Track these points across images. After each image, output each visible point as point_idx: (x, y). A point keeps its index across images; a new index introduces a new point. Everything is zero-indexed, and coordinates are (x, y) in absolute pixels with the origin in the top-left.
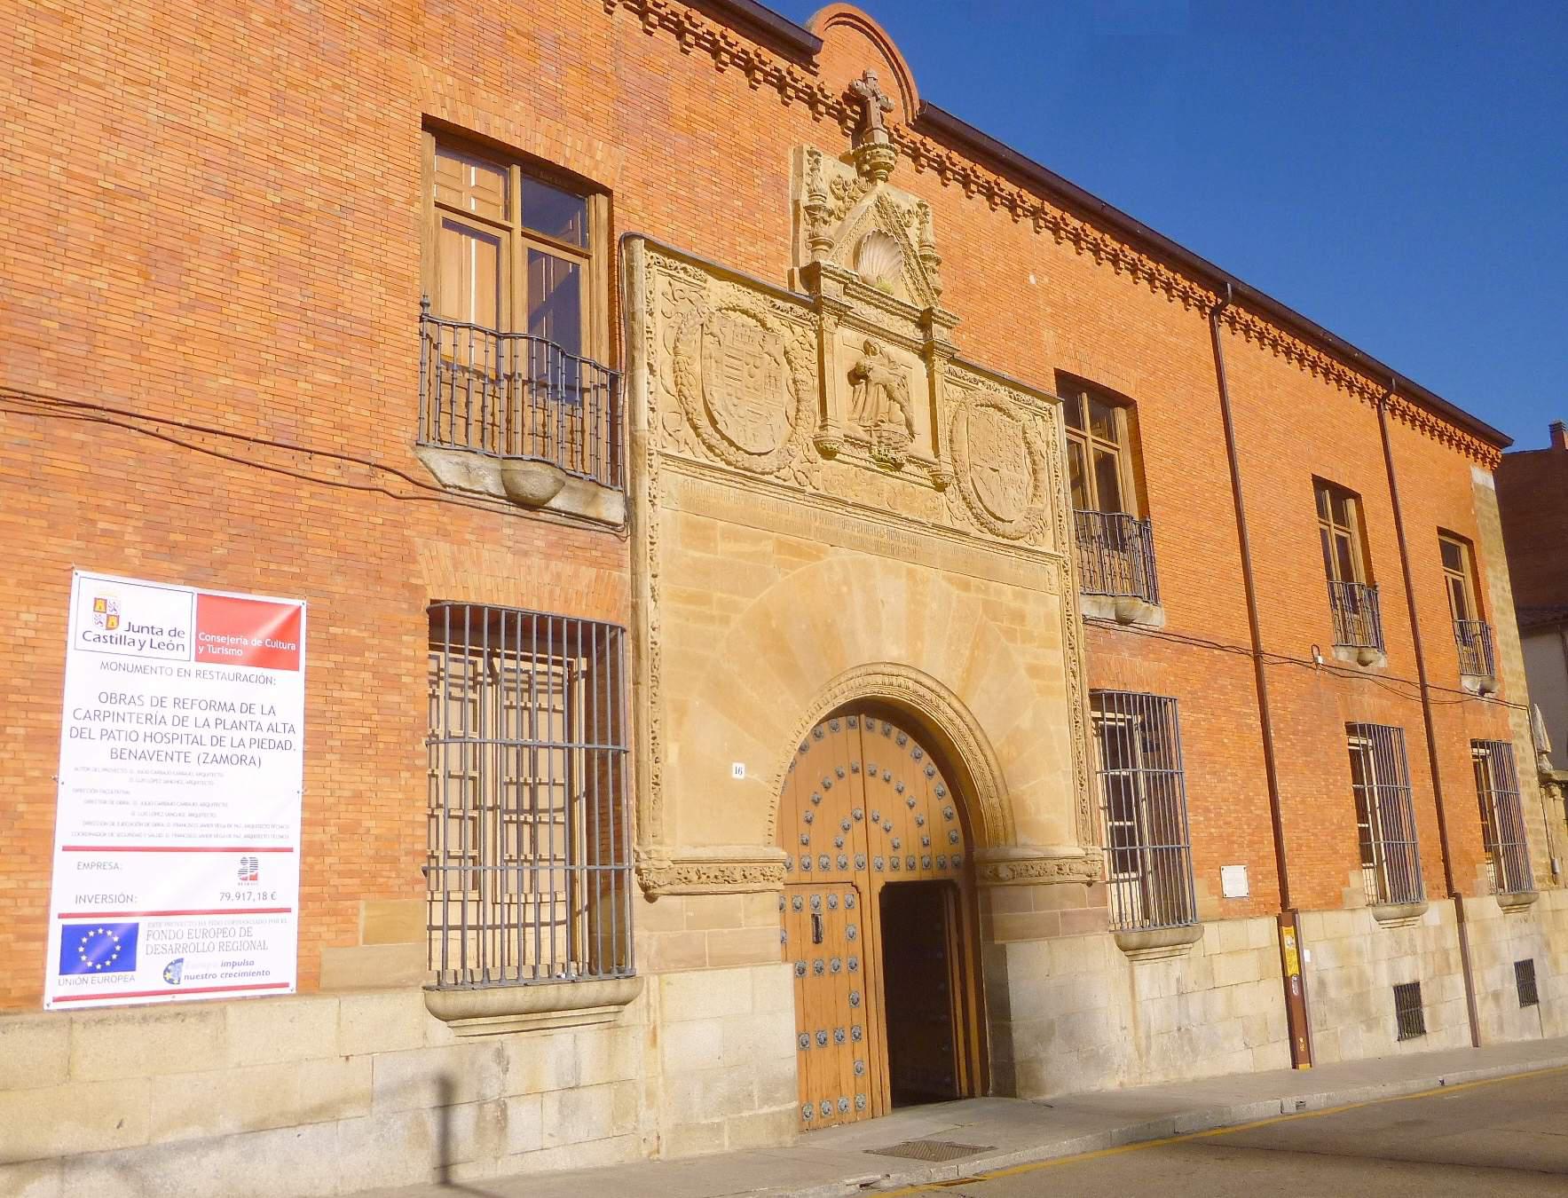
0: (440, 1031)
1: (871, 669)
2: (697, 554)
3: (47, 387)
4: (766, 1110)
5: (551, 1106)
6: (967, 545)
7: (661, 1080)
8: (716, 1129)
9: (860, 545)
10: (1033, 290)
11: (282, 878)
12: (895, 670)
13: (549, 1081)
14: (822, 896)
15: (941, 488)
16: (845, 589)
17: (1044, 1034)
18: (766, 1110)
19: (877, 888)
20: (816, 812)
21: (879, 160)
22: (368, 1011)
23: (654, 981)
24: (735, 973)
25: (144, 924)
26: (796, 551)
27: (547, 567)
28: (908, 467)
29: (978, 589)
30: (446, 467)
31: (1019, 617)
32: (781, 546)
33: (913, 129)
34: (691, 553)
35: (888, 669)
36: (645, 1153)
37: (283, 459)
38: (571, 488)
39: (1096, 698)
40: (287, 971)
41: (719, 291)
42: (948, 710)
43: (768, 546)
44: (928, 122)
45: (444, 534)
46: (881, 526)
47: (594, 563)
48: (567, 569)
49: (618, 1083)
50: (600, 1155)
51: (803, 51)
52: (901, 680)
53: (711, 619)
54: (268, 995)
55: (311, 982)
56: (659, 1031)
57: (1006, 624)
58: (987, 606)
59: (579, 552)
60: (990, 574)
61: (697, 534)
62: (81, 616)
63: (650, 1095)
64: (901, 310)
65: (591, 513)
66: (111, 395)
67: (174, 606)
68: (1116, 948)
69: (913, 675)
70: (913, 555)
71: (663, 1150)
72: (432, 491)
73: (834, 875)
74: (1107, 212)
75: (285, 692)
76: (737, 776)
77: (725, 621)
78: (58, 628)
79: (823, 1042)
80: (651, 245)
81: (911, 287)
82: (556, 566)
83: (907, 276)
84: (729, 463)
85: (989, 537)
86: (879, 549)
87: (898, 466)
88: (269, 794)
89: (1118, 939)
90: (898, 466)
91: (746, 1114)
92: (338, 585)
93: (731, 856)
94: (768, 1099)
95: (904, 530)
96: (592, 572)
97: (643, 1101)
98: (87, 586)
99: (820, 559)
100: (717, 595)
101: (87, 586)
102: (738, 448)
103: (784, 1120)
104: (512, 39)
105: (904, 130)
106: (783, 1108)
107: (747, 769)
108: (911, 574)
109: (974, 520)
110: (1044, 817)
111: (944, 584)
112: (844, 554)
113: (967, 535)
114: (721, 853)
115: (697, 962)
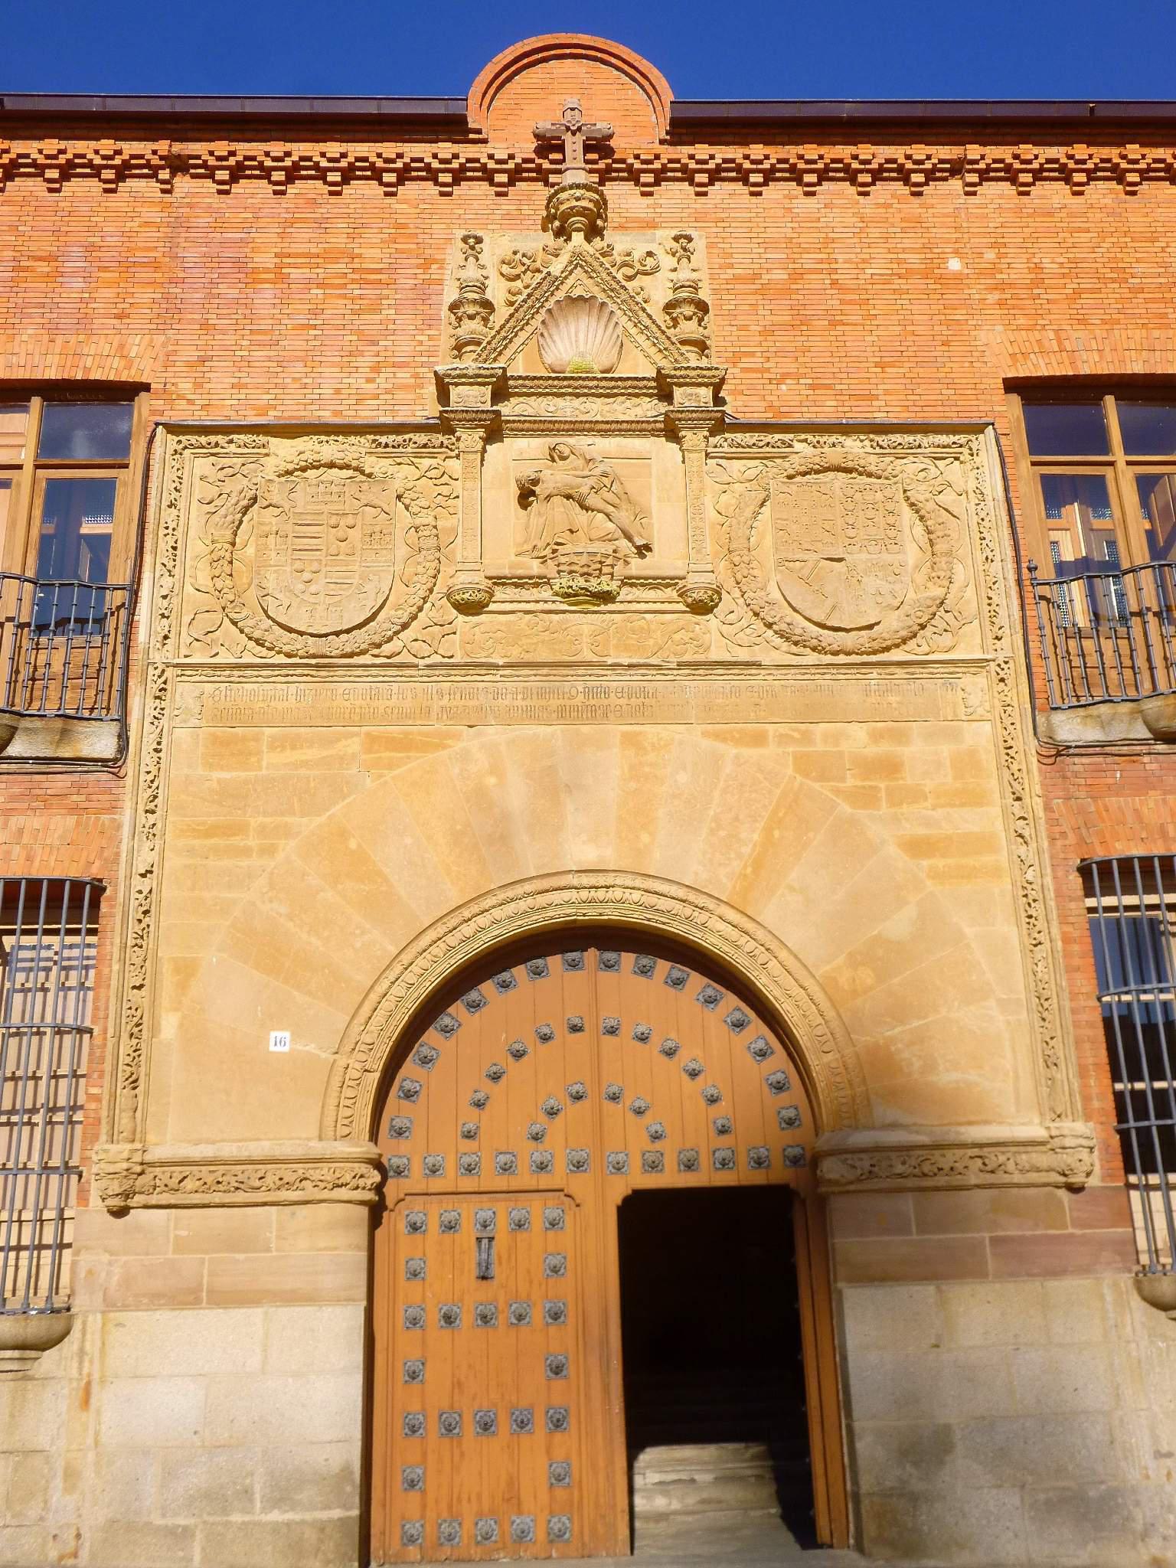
1: (552, 880)
2: (225, 775)
4: (276, 1516)
6: (758, 680)
7: (91, 1456)
10: (958, 277)
12: (601, 880)
15: (701, 608)
16: (492, 780)
17: (925, 1448)
18: (276, 1516)
21: (563, 208)
23: (95, 1321)
24: (238, 1314)
26: (404, 745)
27: (6, 825)
28: (626, 593)
29: (783, 740)
31: (891, 767)
32: (372, 741)
33: (671, 143)
34: (217, 775)
35: (586, 880)
36: (53, 1554)
38: (27, 729)
39: (1098, 875)
41: (284, 451)
42: (721, 926)
43: (353, 746)
47: (75, 810)
48: (35, 822)
51: (454, 127)
52: (618, 893)
53: (246, 852)
56: (95, 1388)
57: (851, 782)
58: (804, 764)
59: (55, 801)
60: (809, 715)
63: (71, 1475)
64: (631, 388)
65: (66, 752)
68: (1136, 1302)
69: (638, 882)
70: (641, 713)
71: (84, 1554)
73: (525, 1178)
74: (1102, 112)
76: (279, 1049)
77: (269, 851)
80: (173, 429)
81: (652, 351)
82: (15, 821)
83: (641, 339)
84: (289, 655)
85: (813, 658)
87: (607, 597)
89: (1138, 1286)
90: (607, 597)
91: (237, 1518)
93: (244, 1154)
94: (281, 1497)
95: (614, 681)
96: (71, 820)
97: (58, 1483)
99: (445, 747)
100: (254, 822)
102: (302, 634)
103: (310, 1535)
104: (26, 269)
105: (668, 152)
106: (308, 1516)
107: (296, 1036)
108: (631, 741)
109: (778, 641)
110: (946, 1077)
111: (706, 743)
112: (493, 733)
113: (758, 665)
114: (229, 1151)
115: (187, 1298)
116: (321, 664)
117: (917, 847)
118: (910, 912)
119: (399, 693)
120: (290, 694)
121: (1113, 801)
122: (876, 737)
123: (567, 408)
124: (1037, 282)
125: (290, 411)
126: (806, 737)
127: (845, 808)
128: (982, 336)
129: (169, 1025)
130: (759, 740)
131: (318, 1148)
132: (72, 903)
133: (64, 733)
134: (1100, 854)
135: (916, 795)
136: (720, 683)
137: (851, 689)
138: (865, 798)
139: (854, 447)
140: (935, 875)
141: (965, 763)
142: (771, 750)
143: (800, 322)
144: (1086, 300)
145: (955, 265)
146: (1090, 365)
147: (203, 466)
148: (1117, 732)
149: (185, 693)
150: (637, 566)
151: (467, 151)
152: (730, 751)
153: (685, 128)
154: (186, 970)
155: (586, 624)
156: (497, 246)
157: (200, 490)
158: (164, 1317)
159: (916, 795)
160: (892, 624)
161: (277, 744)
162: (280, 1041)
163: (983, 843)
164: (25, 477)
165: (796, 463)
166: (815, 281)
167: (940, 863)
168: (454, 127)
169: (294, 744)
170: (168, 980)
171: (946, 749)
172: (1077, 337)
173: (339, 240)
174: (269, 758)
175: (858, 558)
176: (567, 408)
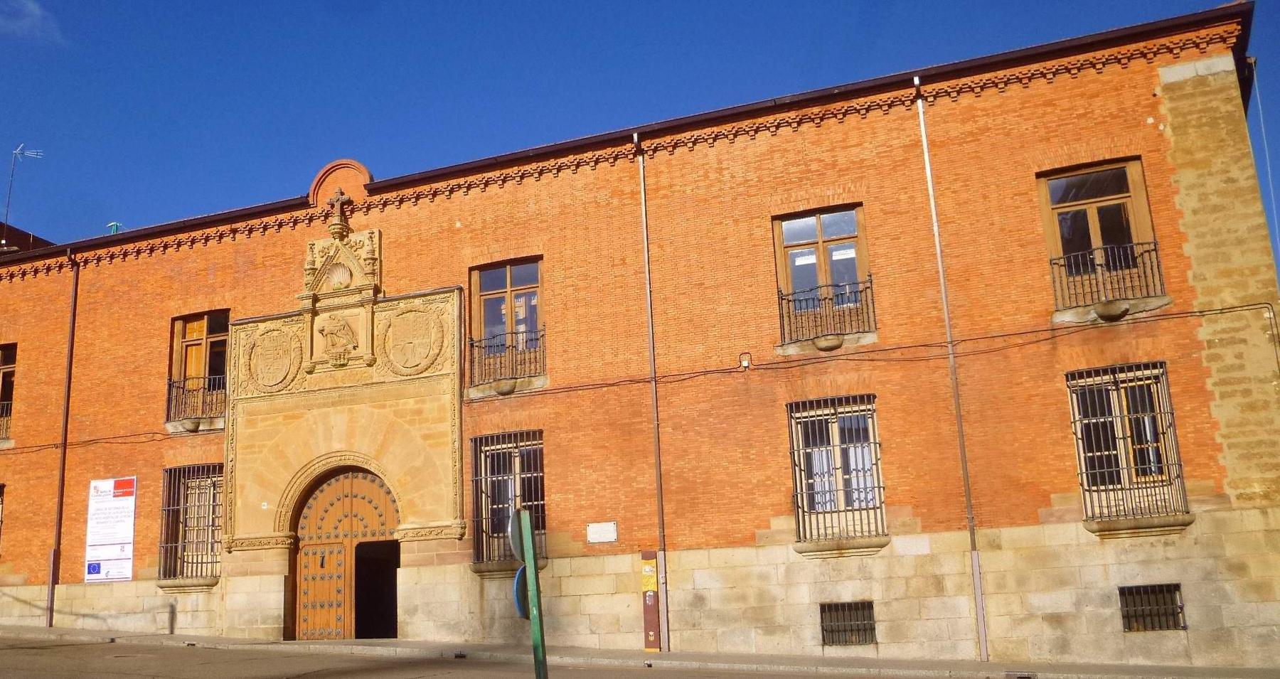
0: (160, 591)
1: (329, 455)
3: (87, 438)
5: (189, 615)
6: (385, 387)
8: (243, 630)
9: (320, 406)
10: (459, 230)
11: (129, 550)
13: (189, 608)
14: (327, 550)
19: (355, 545)
20: (326, 515)
22: (143, 585)
25: (102, 564)
26: (293, 417)
30: (170, 428)
32: (286, 418)
37: (132, 439)
40: (129, 574)
41: (262, 326)
43: (280, 419)
44: (373, 189)
45: (172, 448)
46: (335, 394)
49: (209, 611)
50: (204, 633)
54: (125, 580)
55: (135, 577)
58: (396, 413)
60: (398, 397)
61: (250, 423)
62: (92, 491)
66: (98, 436)
67: (108, 485)
70: (353, 402)
72: (168, 436)
73: (333, 540)
75: (130, 502)
77: (261, 452)
78: (87, 496)
79: (322, 606)
86: (333, 404)
87: (343, 365)
88: (125, 529)
90: (343, 365)
92: (144, 470)
94: (264, 623)
98: (93, 483)
101: (93, 483)
108: (351, 410)
112: (315, 412)
115: (245, 574)
116: (271, 395)
117: (426, 437)
118: (422, 458)
119: (291, 401)
120: (262, 405)
121: (485, 417)
122: (417, 402)
123: (337, 301)
124: (484, 227)
125: (267, 311)
126: (398, 405)
127: (407, 426)
128: (464, 252)
129: (239, 503)
130: (384, 407)
131: (273, 534)
132: (218, 469)
133: (211, 423)
134: (478, 435)
135: (427, 420)
136: (375, 388)
137: (411, 388)
138: (411, 422)
139: (417, 301)
140: (430, 446)
141: (442, 408)
142: (388, 410)
143: (409, 255)
144: (500, 231)
145: (458, 225)
146: (498, 258)
147: (243, 335)
148: (487, 393)
149: (240, 407)
150: (354, 353)
151: (310, 211)
152: (376, 411)
153: (373, 189)
154: (242, 487)
155: (340, 373)
156: (319, 245)
157: (243, 343)
158: (239, 578)
159: (427, 420)
160: (424, 363)
161: (262, 420)
162: (265, 506)
163: (443, 434)
164: (204, 342)
165: (399, 311)
166: (415, 239)
167: (431, 442)
168: (303, 204)
169: (266, 419)
170: (238, 490)
171: (436, 404)
172: (495, 246)
173: (278, 250)
174: (260, 424)
175: (416, 342)
176: (337, 301)
